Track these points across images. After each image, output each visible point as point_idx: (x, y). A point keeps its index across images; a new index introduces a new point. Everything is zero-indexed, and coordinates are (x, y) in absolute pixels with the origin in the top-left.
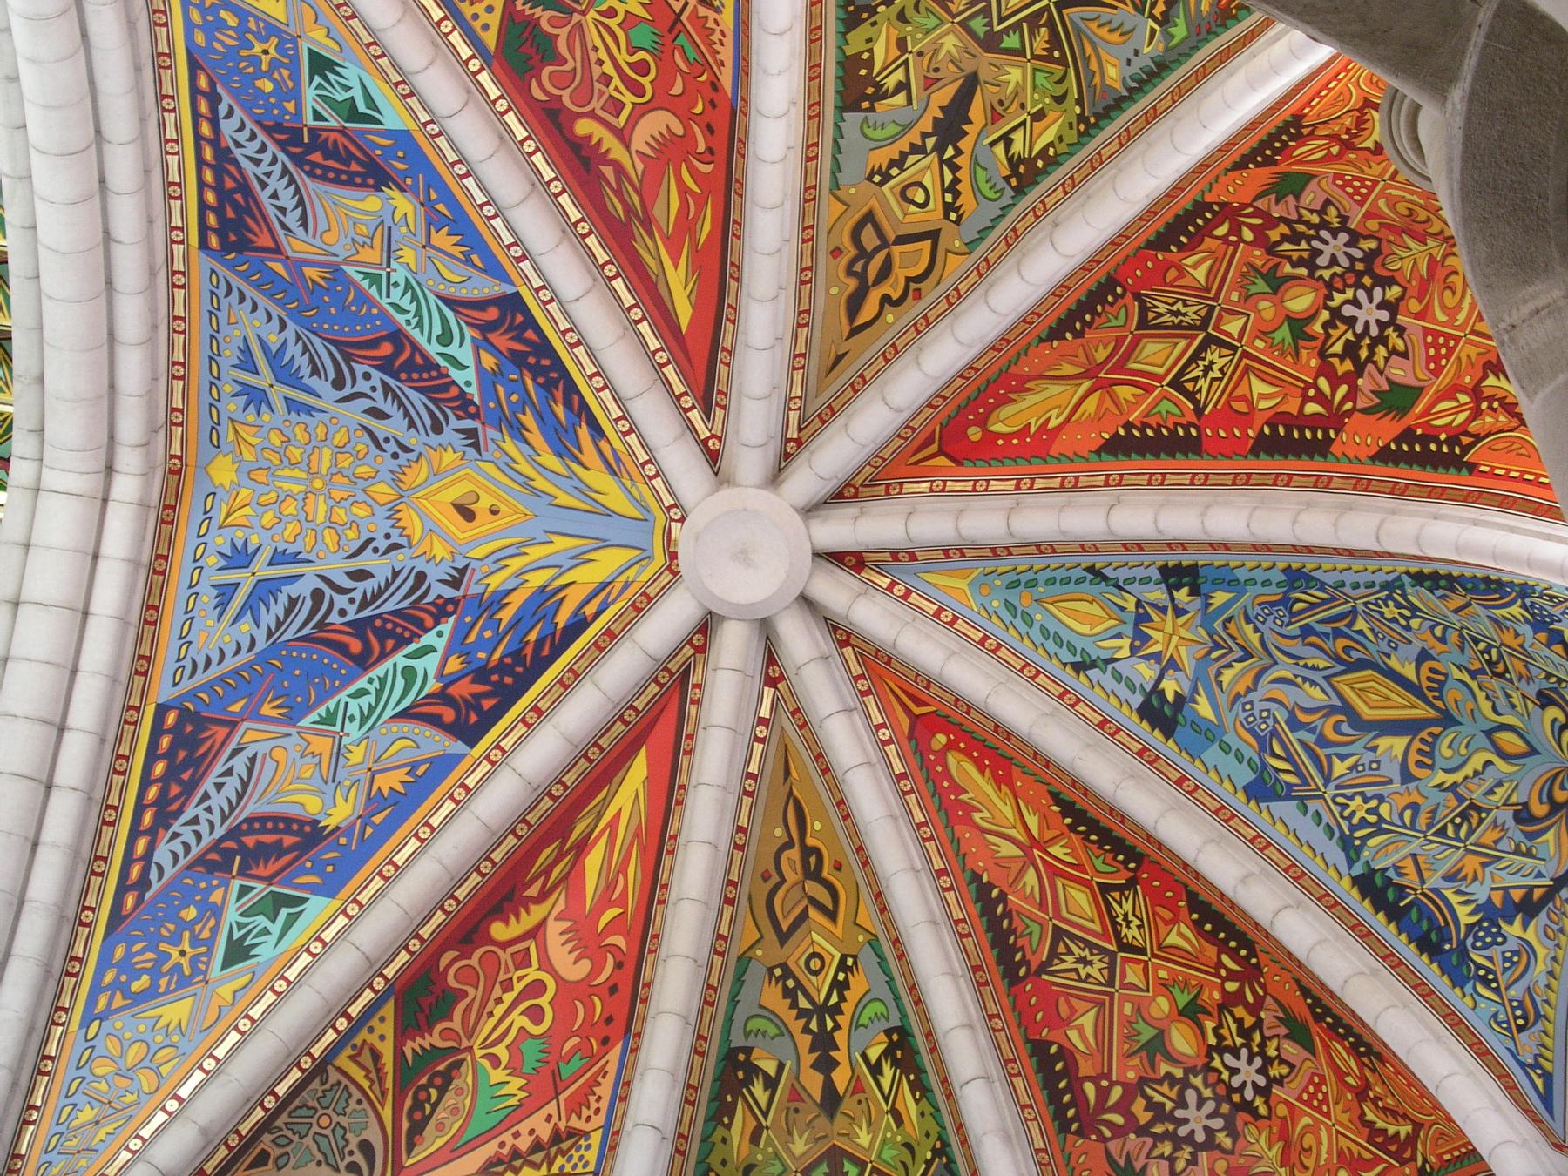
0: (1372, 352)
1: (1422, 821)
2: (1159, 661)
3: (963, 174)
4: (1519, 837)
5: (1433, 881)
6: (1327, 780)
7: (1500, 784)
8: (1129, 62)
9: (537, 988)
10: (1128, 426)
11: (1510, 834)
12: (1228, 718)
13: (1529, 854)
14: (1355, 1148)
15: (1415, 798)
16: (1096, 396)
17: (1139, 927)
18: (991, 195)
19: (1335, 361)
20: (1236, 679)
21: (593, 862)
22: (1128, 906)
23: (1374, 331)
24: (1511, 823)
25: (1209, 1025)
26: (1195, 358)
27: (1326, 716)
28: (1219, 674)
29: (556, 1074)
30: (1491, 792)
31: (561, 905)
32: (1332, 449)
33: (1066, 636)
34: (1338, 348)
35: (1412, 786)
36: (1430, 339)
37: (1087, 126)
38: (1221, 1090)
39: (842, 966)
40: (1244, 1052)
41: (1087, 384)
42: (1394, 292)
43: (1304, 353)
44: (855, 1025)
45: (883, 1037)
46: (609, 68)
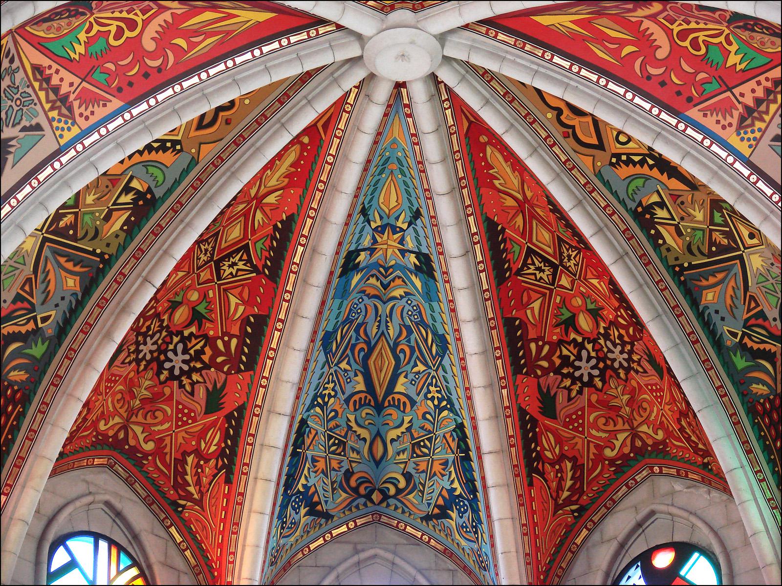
0: (565, 376)
1: (332, 424)
2: (373, 244)
3: (638, 169)
4: (339, 480)
5: (309, 453)
6: (336, 365)
7: (358, 453)
8: (717, 312)
9: (132, 25)
10: (503, 229)
11: (339, 473)
12: (354, 295)
13: (333, 490)
14: (167, 450)
15: (340, 411)
16: (515, 204)
17: (231, 273)
18: (630, 191)
19: (558, 353)
20: (373, 286)
21: (208, 15)
22: (241, 265)
23: (577, 374)
24: (343, 470)
25: (193, 329)
26: (545, 260)
27: (365, 342)
28: (372, 276)
29: (92, 70)
30: (353, 449)
31: (179, 12)
32: (519, 376)
33: (376, 194)
34: (565, 352)
35: (345, 406)
36: (580, 413)
37: (677, 272)
38: (163, 347)
39: (175, 143)
40: (187, 357)
41: (520, 197)
42: (600, 384)
43: (558, 330)
44: (146, 164)
45: (146, 187)
46: (693, 25)
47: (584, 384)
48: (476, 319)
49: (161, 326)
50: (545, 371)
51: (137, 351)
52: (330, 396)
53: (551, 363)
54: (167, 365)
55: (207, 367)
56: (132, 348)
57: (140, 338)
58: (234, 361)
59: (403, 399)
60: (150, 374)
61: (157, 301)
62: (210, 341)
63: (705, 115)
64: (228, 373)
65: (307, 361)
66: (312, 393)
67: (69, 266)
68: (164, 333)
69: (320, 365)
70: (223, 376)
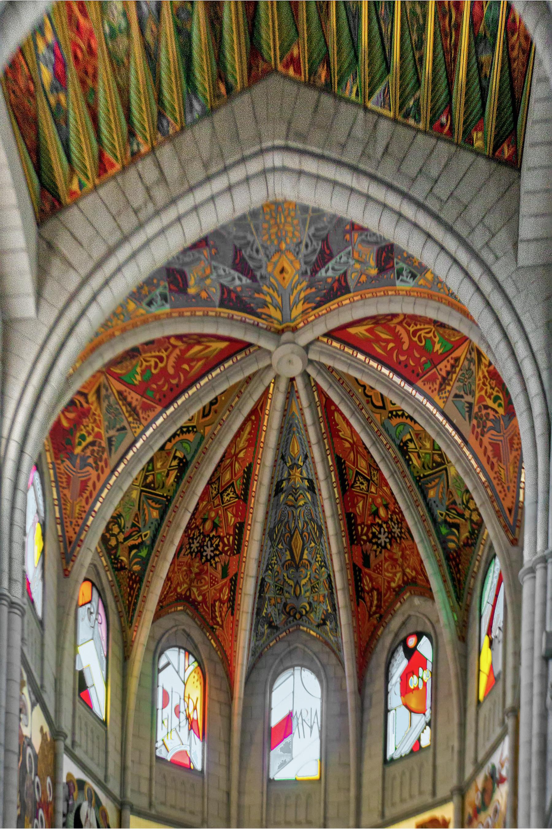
0: (374, 544)
23: (379, 542)
40: (212, 549)
42: (389, 546)
47: (383, 548)
48: (333, 516)
49: (199, 533)
50: (365, 542)
51: (190, 548)
52: (275, 564)
53: (368, 537)
54: (205, 554)
55: (221, 553)
56: (188, 547)
57: (191, 541)
58: (231, 549)
59: (307, 562)
60: (198, 559)
61: (196, 519)
62: (221, 539)
63: (424, 384)
64: (230, 556)
65: (262, 546)
66: (266, 563)
67: (153, 504)
68: (202, 537)
69: (269, 546)
70: (228, 557)
